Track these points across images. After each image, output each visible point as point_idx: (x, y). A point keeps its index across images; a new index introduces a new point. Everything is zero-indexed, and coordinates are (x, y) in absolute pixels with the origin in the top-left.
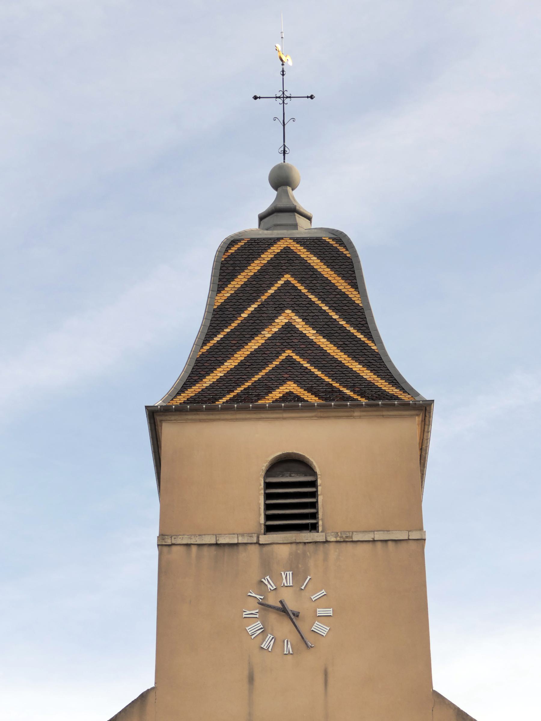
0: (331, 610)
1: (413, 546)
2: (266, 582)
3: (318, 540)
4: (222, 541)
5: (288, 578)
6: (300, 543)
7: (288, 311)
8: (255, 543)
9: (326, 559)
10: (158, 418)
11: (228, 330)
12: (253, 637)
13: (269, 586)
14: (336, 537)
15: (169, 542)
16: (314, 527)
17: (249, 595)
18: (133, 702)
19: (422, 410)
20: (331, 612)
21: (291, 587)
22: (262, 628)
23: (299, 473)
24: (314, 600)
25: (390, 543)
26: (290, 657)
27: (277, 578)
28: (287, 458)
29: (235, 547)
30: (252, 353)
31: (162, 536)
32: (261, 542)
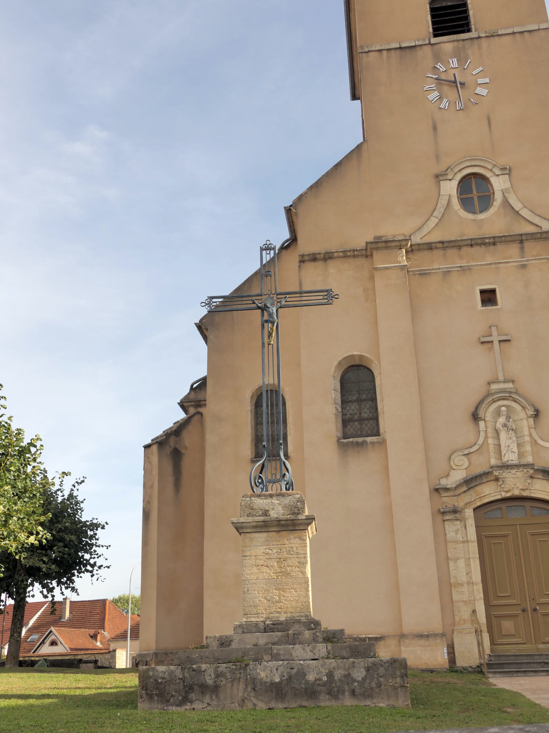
0: (488, 79)
1: (542, 33)
2: (439, 67)
3: (473, 36)
4: (404, 45)
5: (454, 63)
6: (460, 40)
8: (427, 44)
9: (480, 48)
12: (433, 102)
13: (441, 69)
14: (486, 34)
15: (367, 50)
16: (469, 30)
17: (427, 77)
18: (352, 151)
20: (488, 80)
21: (457, 69)
22: (439, 96)
24: (474, 74)
25: (525, 33)
29: (414, 48)
32: (432, 43)
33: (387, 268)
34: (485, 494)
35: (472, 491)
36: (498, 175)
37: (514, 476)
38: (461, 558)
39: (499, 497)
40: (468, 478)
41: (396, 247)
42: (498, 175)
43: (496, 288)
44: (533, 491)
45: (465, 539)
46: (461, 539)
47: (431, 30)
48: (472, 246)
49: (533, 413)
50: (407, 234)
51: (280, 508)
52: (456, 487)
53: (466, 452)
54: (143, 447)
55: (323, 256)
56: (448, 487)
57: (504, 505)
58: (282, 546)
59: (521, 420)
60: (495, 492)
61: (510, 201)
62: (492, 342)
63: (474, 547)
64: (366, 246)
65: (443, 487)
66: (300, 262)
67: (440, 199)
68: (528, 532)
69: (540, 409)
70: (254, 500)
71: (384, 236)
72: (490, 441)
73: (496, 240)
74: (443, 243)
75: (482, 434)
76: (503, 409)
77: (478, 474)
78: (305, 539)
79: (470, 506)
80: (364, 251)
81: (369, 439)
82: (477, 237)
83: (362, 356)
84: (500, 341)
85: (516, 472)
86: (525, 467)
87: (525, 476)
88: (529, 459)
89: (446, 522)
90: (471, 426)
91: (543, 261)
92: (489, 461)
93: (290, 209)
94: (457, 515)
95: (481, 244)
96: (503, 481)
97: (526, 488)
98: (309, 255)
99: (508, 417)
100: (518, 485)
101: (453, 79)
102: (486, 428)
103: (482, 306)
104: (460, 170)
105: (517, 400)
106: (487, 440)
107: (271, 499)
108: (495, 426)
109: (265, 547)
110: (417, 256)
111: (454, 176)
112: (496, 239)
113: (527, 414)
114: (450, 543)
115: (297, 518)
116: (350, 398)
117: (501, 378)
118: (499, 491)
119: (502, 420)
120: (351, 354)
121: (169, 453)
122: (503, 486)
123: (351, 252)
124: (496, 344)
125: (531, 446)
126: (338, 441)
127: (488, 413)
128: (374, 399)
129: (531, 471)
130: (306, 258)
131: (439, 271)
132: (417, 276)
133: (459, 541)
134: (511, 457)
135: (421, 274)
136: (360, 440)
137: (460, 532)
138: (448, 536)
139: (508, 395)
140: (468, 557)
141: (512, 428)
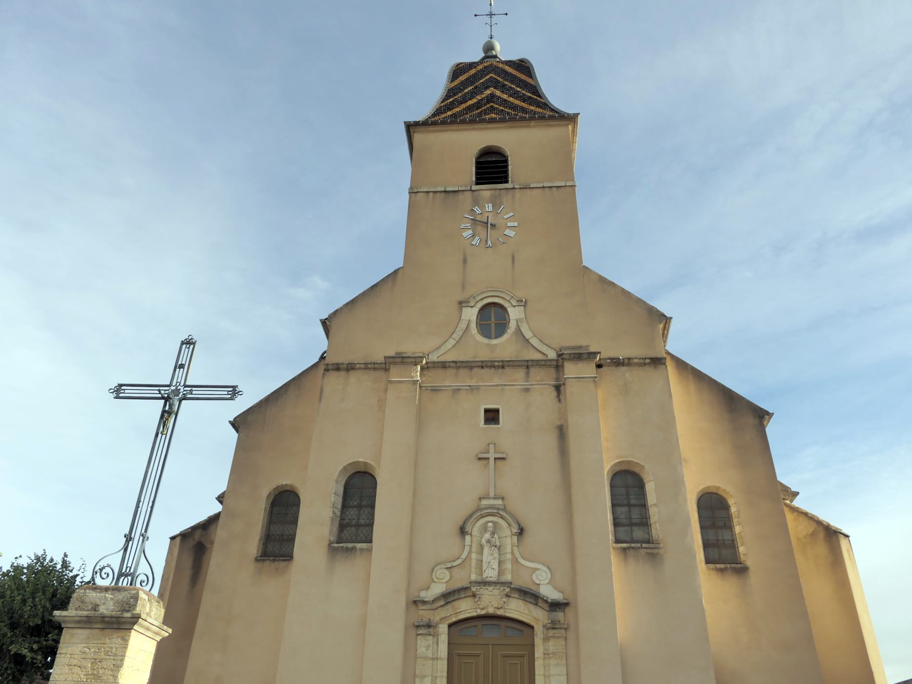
2: (476, 210)
5: (489, 207)
6: (497, 189)
8: (469, 190)
9: (513, 197)
10: (411, 130)
13: (477, 212)
15: (416, 191)
16: (507, 182)
19: (572, 121)
25: (554, 188)
26: (490, 248)
27: (482, 207)
28: (490, 151)
31: (411, 188)
33: (400, 382)
34: (460, 610)
35: (449, 606)
36: (514, 306)
37: (490, 593)
38: (428, 676)
39: (474, 614)
40: (447, 592)
41: (411, 363)
42: (514, 306)
43: (499, 408)
44: (508, 611)
45: (435, 656)
46: (431, 656)
47: (474, 179)
48: (482, 367)
49: (517, 531)
50: (426, 352)
51: (111, 603)
52: (433, 601)
53: (449, 565)
54: (170, 538)
55: (345, 366)
56: (425, 600)
57: (479, 623)
58: (102, 645)
59: (505, 537)
60: (471, 609)
62: (488, 458)
63: (443, 666)
64: (385, 360)
65: (421, 599)
66: (325, 370)
67: (460, 323)
68: (499, 653)
69: (525, 528)
70: (89, 593)
71: (405, 353)
72: (474, 556)
74: (456, 362)
75: (467, 548)
76: (490, 524)
77: (456, 589)
78: (127, 639)
79: (445, 621)
80: (384, 365)
81: (359, 545)
82: (487, 360)
83: (367, 463)
84: (495, 459)
85: (493, 589)
86: (503, 585)
87: (502, 594)
88: (508, 577)
89: (419, 637)
90: (457, 539)
91: (545, 386)
92: (470, 577)
93: (325, 322)
94: (431, 630)
95: (491, 367)
96: (480, 598)
97: (500, 606)
98: (333, 364)
99: (493, 534)
100: (493, 603)
101: (486, 221)
102: (471, 543)
103: (485, 424)
104: (482, 299)
105: (504, 517)
106: (471, 555)
107: (106, 593)
108: (481, 541)
109: (83, 645)
110: (431, 373)
111: (475, 304)
112: (504, 363)
113: (512, 532)
114: (419, 659)
115: (122, 616)
116: (351, 504)
117: (492, 494)
118: (475, 607)
119: (487, 536)
120: (356, 460)
121: (192, 546)
122: (479, 603)
123: (372, 365)
124: (492, 461)
125: (512, 564)
126: (329, 545)
127: (475, 529)
128: (373, 506)
129: (508, 590)
130: (330, 367)
131: (449, 388)
132: (428, 391)
133: (428, 657)
134: (491, 574)
135: (432, 390)
136: (350, 545)
137: (431, 648)
138: (418, 651)
139: (495, 512)
140: (436, 675)
141: (495, 544)
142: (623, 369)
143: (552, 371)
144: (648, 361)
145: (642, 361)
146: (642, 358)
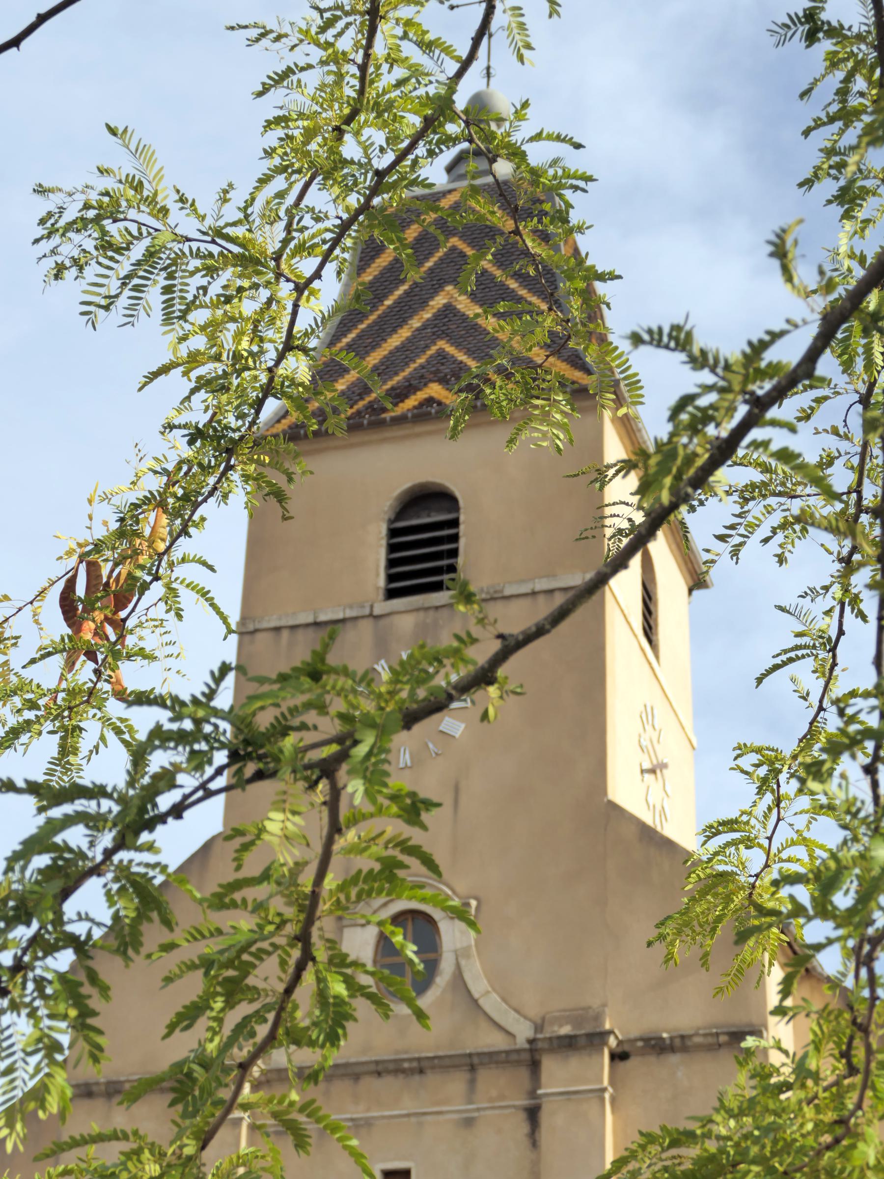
2: (379, 669)
4: (323, 618)
7: (449, 288)
11: (362, 326)
15: (251, 627)
23: (440, 511)
26: (407, 772)
30: (391, 353)
47: (382, 581)
55: (103, 1088)
61: (467, 976)
73: (424, 1064)
142: (674, 1059)
143: (524, 1074)
144: (723, 1039)
145: (710, 1040)
146: (711, 1035)
